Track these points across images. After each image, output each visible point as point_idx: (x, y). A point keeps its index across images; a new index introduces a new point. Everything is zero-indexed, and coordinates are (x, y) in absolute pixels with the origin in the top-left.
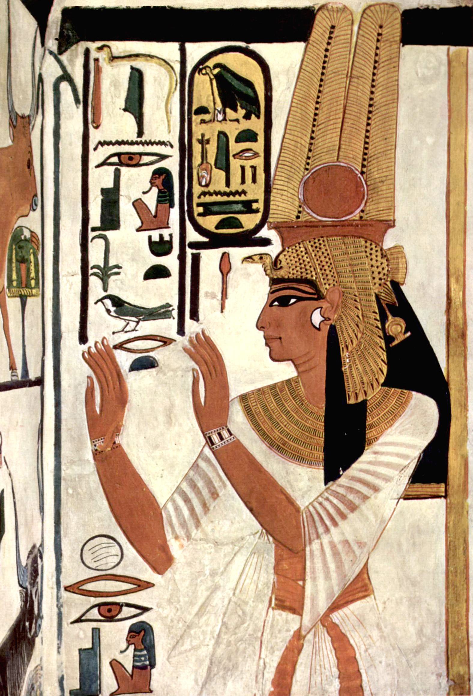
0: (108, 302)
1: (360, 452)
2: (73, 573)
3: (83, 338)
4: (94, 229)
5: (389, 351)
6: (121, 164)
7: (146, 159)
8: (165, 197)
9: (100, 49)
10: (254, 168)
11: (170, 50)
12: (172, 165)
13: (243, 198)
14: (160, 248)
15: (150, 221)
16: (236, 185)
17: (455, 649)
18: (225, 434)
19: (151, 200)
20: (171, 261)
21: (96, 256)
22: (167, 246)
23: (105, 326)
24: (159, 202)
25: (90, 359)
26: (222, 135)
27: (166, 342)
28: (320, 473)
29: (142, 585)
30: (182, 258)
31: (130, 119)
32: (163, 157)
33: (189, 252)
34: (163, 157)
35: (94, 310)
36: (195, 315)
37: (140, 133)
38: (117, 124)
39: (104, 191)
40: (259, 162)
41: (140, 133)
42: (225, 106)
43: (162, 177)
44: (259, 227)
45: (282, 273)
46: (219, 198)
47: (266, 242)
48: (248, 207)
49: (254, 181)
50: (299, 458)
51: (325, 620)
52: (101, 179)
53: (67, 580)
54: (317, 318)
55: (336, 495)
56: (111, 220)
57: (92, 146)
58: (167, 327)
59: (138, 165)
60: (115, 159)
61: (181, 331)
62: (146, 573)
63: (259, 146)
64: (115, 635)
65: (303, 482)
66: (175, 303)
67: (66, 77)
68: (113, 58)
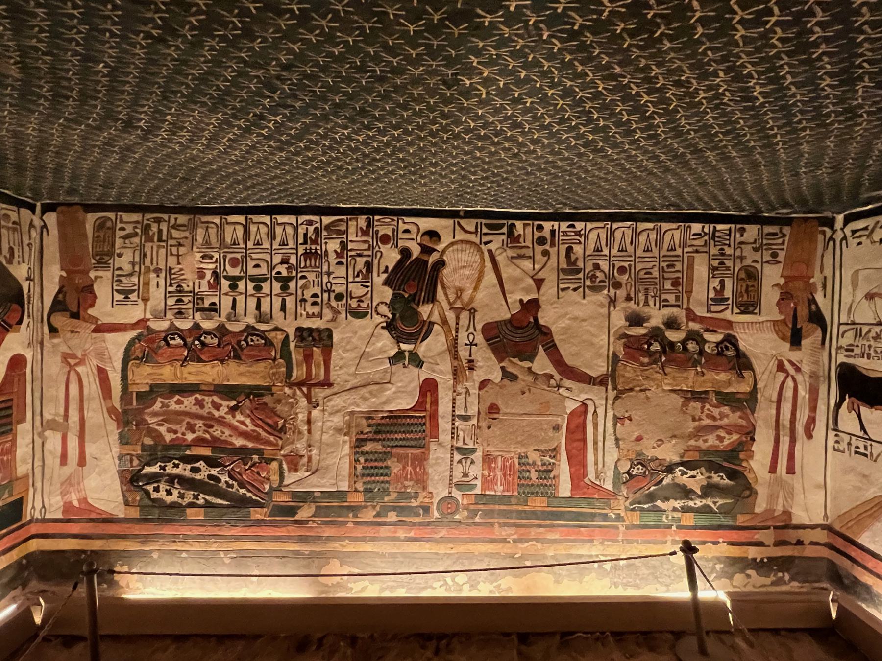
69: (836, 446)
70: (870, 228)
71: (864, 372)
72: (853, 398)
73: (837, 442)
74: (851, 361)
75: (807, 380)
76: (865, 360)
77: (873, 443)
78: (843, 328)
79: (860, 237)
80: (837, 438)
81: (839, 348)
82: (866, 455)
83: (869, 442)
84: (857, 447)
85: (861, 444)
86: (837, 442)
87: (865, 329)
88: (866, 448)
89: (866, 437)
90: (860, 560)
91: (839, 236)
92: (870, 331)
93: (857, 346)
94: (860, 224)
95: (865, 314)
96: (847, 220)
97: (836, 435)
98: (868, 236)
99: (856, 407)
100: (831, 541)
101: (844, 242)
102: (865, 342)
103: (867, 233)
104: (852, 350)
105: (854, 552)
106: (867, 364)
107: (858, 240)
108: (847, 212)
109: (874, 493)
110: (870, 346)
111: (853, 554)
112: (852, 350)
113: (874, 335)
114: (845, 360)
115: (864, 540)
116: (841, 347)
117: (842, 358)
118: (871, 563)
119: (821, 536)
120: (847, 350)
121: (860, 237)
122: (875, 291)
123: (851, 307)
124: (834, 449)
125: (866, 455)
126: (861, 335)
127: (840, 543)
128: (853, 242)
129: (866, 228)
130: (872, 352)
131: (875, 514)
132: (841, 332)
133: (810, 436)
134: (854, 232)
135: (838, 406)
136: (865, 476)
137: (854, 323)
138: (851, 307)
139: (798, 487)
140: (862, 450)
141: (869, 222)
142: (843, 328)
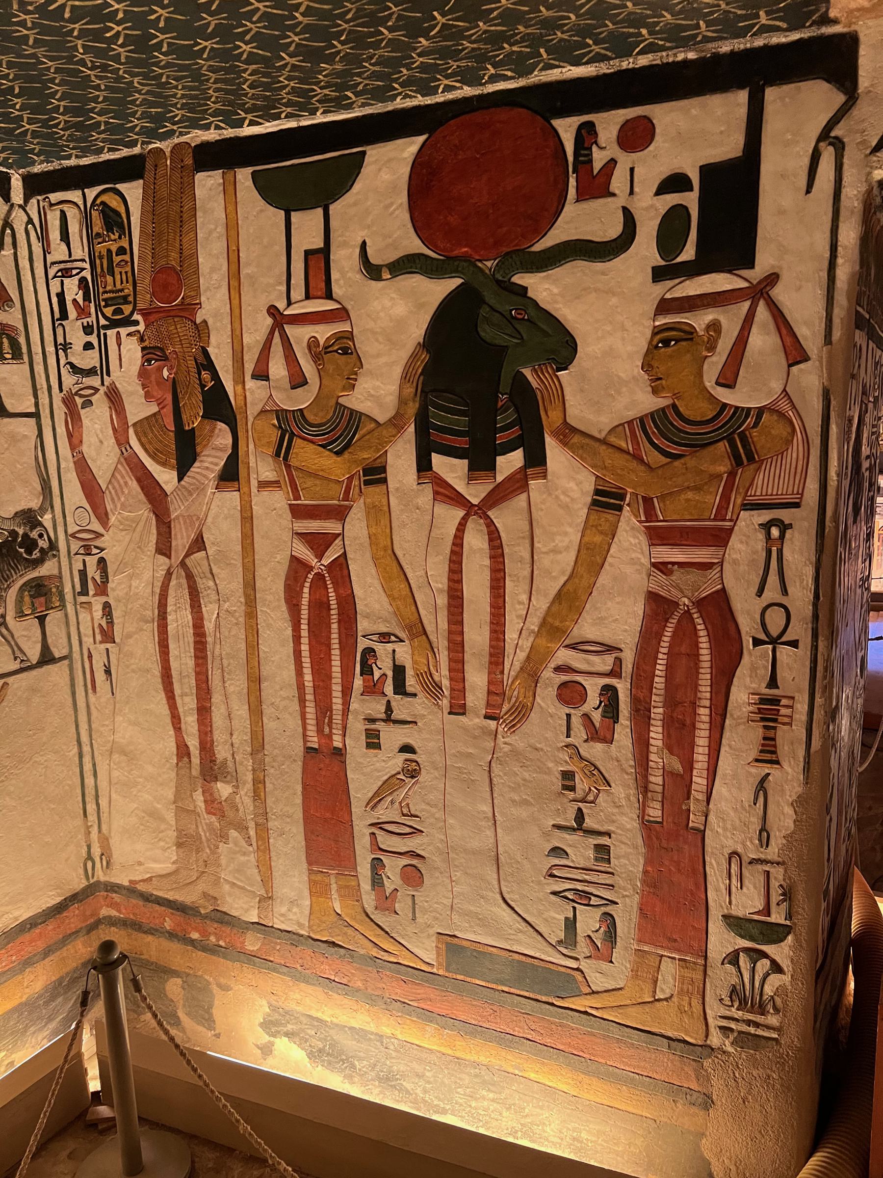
0: (68, 366)
1: (194, 461)
3: (61, 390)
4: (58, 320)
5: (203, 392)
6: (63, 276)
7: (74, 272)
8: (86, 297)
9: (44, 199)
10: (126, 273)
11: (75, 196)
12: (87, 274)
13: (123, 294)
14: (88, 330)
15: (82, 312)
16: (119, 286)
18: (128, 448)
19: (80, 298)
20: (93, 339)
22: (90, 329)
23: (69, 380)
24: (84, 300)
25: (64, 401)
26: (109, 251)
27: (97, 390)
28: (175, 474)
29: (99, 535)
31: (64, 246)
32: (83, 269)
33: (102, 332)
34: (83, 269)
35: (63, 371)
36: (108, 374)
37: (70, 256)
38: (59, 252)
39: (58, 295)
40: (129, 269)
41: (70, 256)
42: (108, 232)
43: (83, 282)
44: (132, 313)
45: (146, 343)
46: (111, 295)
47: (136, 323)
48: (125, 300)
49: (127, 282)
50: (164, 464)
51: (183, 564)
52: (55, 287)
53: (70, 531)
54: (165, 373)
55: (184, 487)
56: (64, 315)
57: (48, 266)
58: (95, 381)
59: (71, 276)
60: (60, 274)
61: (103, 384)
62: (101, 530)
63: (127, 257)
64: (92, 562)
65: (166, 477)
66: (98, 365)
67: (30, 221)
68: (51, 205)
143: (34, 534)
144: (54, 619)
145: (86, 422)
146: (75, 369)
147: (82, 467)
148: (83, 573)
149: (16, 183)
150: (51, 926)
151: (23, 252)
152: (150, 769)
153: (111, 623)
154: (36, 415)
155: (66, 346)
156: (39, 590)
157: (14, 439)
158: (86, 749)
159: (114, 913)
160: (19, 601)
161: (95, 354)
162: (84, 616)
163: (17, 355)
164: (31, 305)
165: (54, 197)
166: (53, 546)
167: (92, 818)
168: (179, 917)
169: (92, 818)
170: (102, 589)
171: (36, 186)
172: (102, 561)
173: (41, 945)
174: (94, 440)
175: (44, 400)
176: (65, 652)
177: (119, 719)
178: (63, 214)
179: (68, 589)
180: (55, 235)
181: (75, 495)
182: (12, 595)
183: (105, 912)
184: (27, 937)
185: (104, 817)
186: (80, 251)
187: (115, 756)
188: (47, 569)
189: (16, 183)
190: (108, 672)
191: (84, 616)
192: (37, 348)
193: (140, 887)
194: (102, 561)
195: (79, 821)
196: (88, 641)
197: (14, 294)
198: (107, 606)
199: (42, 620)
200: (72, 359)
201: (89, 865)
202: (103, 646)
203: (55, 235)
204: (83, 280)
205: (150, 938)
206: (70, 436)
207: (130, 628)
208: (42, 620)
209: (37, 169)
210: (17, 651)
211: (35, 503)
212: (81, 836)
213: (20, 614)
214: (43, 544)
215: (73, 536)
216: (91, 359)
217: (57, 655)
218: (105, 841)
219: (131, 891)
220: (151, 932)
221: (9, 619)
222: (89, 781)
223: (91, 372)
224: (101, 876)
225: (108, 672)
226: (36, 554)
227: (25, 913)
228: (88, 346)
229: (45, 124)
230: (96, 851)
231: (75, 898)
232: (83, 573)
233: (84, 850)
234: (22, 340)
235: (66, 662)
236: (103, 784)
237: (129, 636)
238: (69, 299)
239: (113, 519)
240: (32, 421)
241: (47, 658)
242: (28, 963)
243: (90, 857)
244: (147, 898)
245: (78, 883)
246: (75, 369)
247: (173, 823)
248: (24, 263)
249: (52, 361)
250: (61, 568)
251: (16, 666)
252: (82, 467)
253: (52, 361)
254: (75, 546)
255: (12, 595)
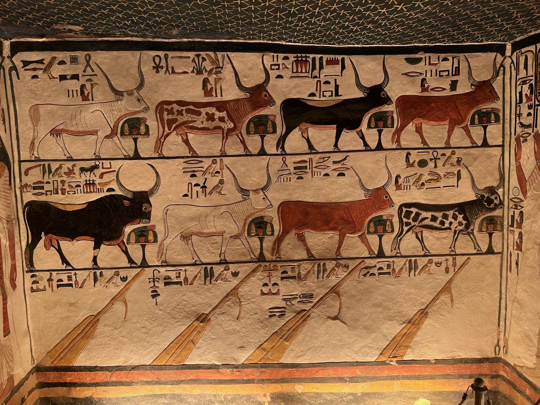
2: (511, 196)
3: (515, 134)
6: (523, 84)
8: (531, 93)
11: (532, 48)
12: (533, 82)
14: (530, 107)
15: (529, 99)
17: (5, 299)
20: (532, 111)
21: (518, 112)
23: (519, 130)
24: (530, 94)
27: (530, 134)
29: (522, 201)
30: (534, 110)
31: (525, 71)
33: (536, 107)
35: (517, 126)
36: (536, 127)
37: (527, 75)
38: (523, 73)
39: (519, 93)
43: (531, 86)
52: (519, 90)
53: (510, 197)
56: (521, 101)
58: (530, 130)
61: (533, 131)
62: (523, 198)
64: (517, 212)
66: (532, 123)
67: (513, 62)
68: (522, 53)
69: (35, 287)
70: (46, 62)
71: (61, 207)
72: (50, 235)
73: (34, 283)
74: (42, 198)
75: (6, 226)
76: (60, 196)
77: (77, 272)
78: (25, 166)
79: (34, 69)
80: (34, 279)
81: (22, 187)
82: (71, 285)
83: (73, 272)
84: (61, 280)
85: (64, 277)
86: (34, 283)
87: (54, 166)
88: (70, 278)
89: (70, 268)
90: (77, 381)
91: (7, 64)
92: (60, 167)
93: (48, 183)
94: (34, 56)
95: (51, 150)
96: (16, 48)
97: (32, 276)
98: (45, 70)
99: (55, 243)
100: (42, 380)
101: (14, 72)
102: (56, 178)
103: (43, 66)
104: (42, 188)
105: (69, 378)
106: (63, 199)
107: (34, 73)
108: (13, 40)
109: (82, 316)
110: (63, 182)
111: (68, 380)
112: (42, 188)
113: (67, 171)
114: (34, 198)
115: (81, 361)
116: (26, 185)
117: (29, 197)
118: (88, 377)
119: (33, 381)
120: (35, 188)
121: (34, 69)
122: (61, 127)
123: (33, 143)
124: (33, 290)
125: (71, 285)
126: (50, 171)
127: (53, 377)
128: (26, 75)
129: (41, 62)
130: (66, 186)
131: (88, 334)
132: (23, 171)
133: (14, 286)
134: (26, 63)
135: (31, 247)
136: (71, 304)
137: (38, 160)
138: (33, 143)
139: (14, 345)
140: (66, 281)
141: (46, 56)
142: (25, 166)
143: (493, 197)
144: (496, 235)
145: (523, 149)
146: (522, 125)
147: (519, 169)
148: (513, 217)
149: (509, 47)
150: (474, 366)
151: (508, 76)
152: (530, 315)
153: (521, 242)
154: (502, 146)
155: (520, 115)
156: (491, 221)
157: (489, 156)
158: (503, 296)
159: (505, 375)
160: (481, 225)
161: (531, 118)
162: (510, 236)
163: (497, 120)
164: (507, 98)
165: (523, 50)
166: (501, 203)
167: (502, 328)
168: (533, 392)
169: (502, 328)
170: (520, 226)
171: (516, 47)
172: (521, 213)
173: (468, 372)
174: (526, 157)
175: (507, 139)
176: (500, 251)
177: (519, 287)
178: (526, 56)
179: (505, 223)
180: (522, 66)
181: (514, 181)
182: (478, 222)
183: (502, 373)
184: (463, 365)
185: (507, 329)
186: (531, 72)
187: (515, 304)
188: (497, 213)
189: (509, 47)
190: (517, 264)
191: (510, 236)
192: (507, 117)
193: (518, 368)
194: (521, 213)
195: (496, 327)
196: (511, 248)
197: (500, 95)
198: (520, 234)
199: (490, 235)
200: (522, 121)
201: (497, 349)
202: (517, 252)
203: (522, 66)
204: (532, 84)
205: (518, 395)
206: (516, 155)
207: (529, 246)
208: (490, 235)
209: (518, 39)
210: (476, 245)
211: (495, 184)
212: (495, 334)
213: (480, 230)
214: (496, 202)
215: (511, 200)
216: (529, 121)
217: (496, 251)
218: (506, 341)
219: (514, 368)
220: (519, 391)
221: (475, 232)
222: (503, 311)
223: (529, 126)
224: (502, 355)
225: (517, 264)
226: (492, 206)
227: (464, 355)
228: (529, 114)
229: (514, 23)
230: (502, 344)
231: (487, 360)
232: (513, 217)
233: (496, 342)
234: (501, 114)
235: (500, 255)
236: (509, 315)
237: (528, 250)
238: (524, 94)
239: (529, 194)
240: (500, 149)
241: (490, 251)
242: (461, 376)
243: (498, 345)
244: (521, 376)
245: (491, 354)
246: (522, 125)
247: (537, 345)
248: (507, 81)
249: (513, 122)
250: (505, 213)
251: (475, 251)
252: (519, 169)
253: (513, 122)
254: (512, 204)
255: (478, 222)
